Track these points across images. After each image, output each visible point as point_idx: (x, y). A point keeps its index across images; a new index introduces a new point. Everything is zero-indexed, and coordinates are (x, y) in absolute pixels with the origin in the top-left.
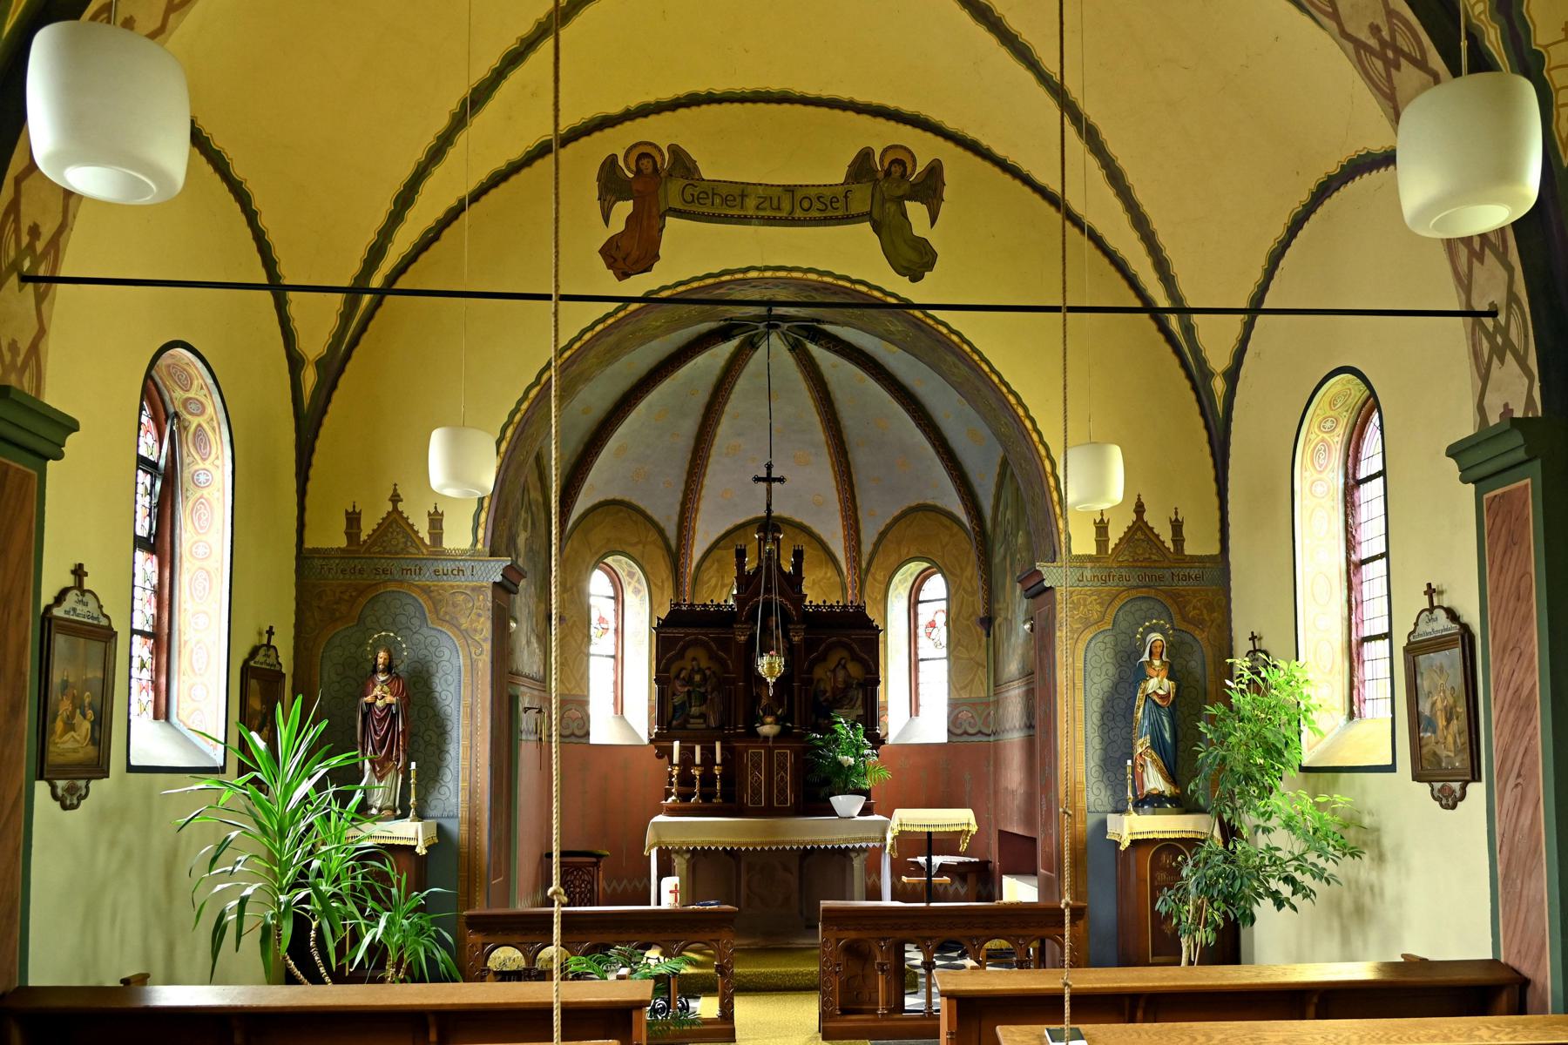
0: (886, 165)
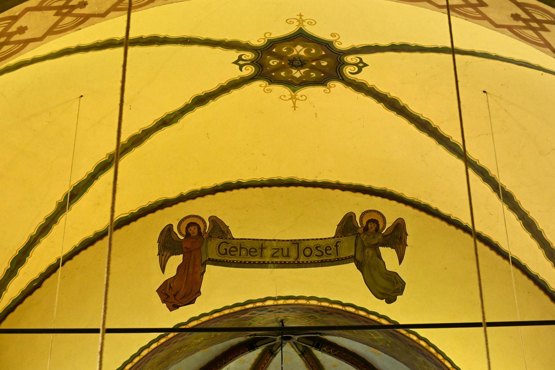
0: (364, 223)
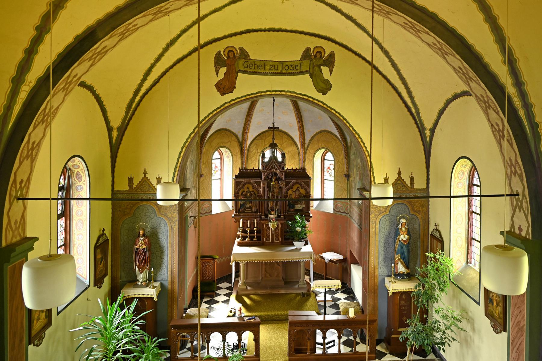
0: (315, 53)
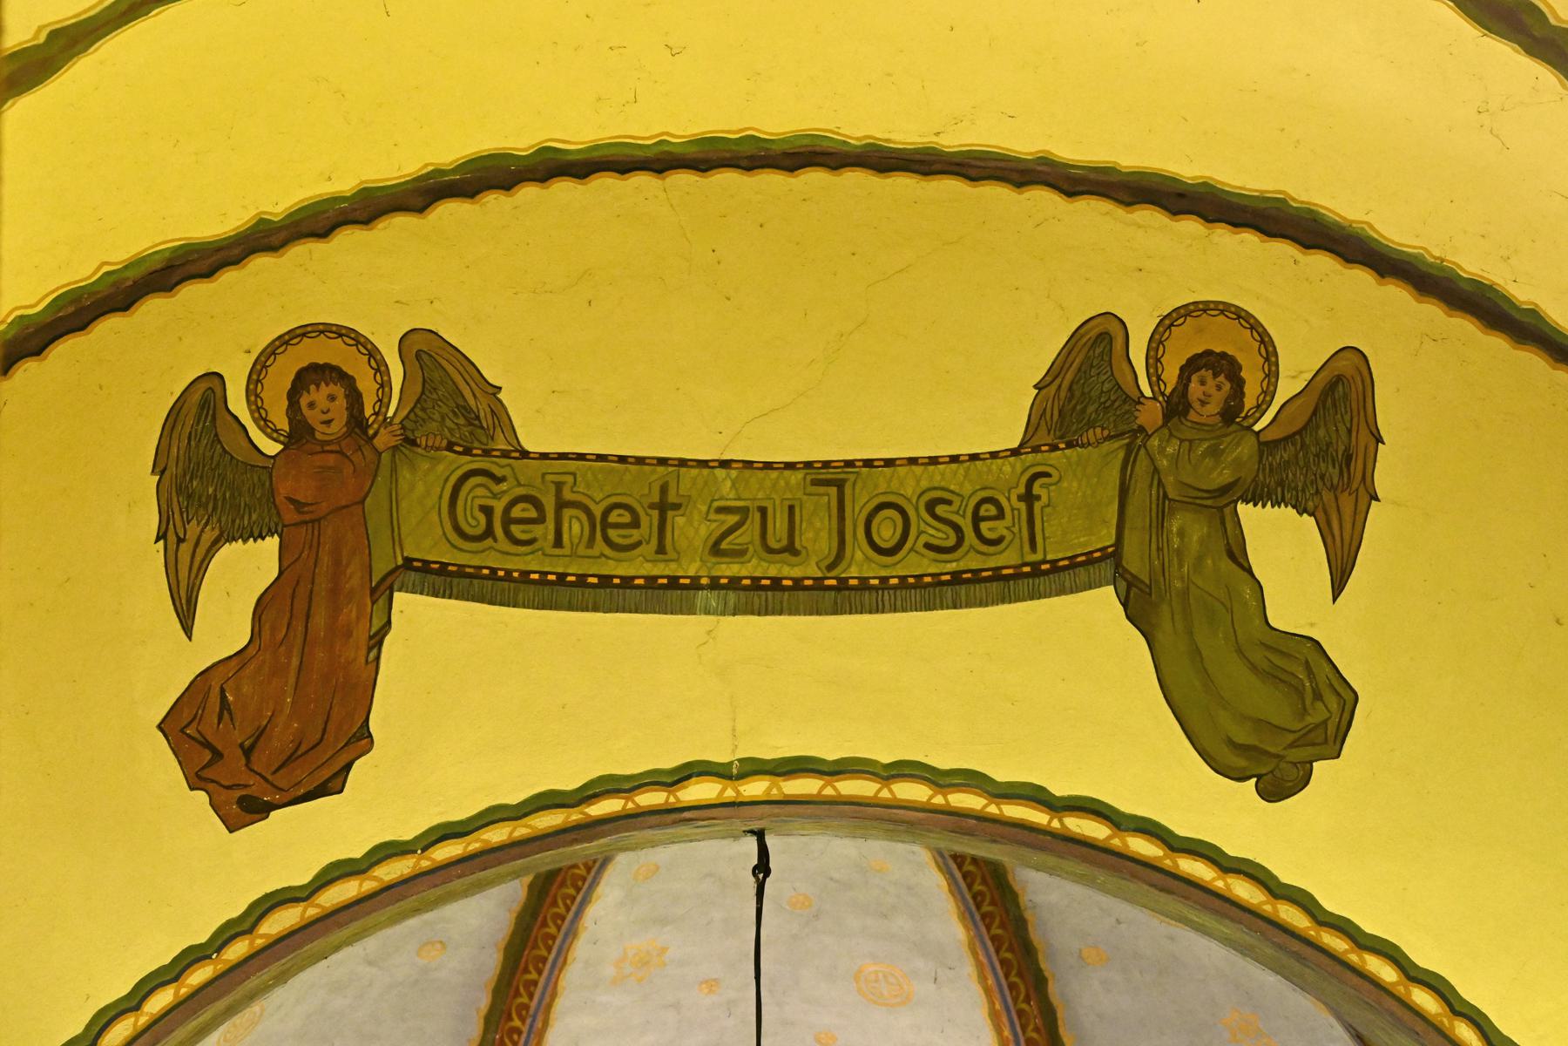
0: (1171, 375)
